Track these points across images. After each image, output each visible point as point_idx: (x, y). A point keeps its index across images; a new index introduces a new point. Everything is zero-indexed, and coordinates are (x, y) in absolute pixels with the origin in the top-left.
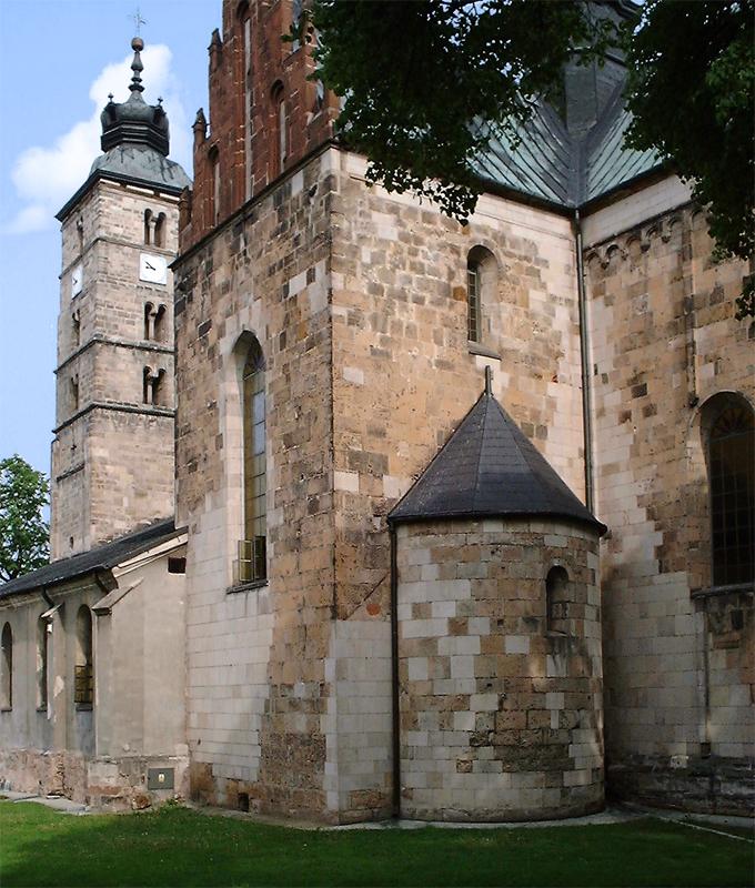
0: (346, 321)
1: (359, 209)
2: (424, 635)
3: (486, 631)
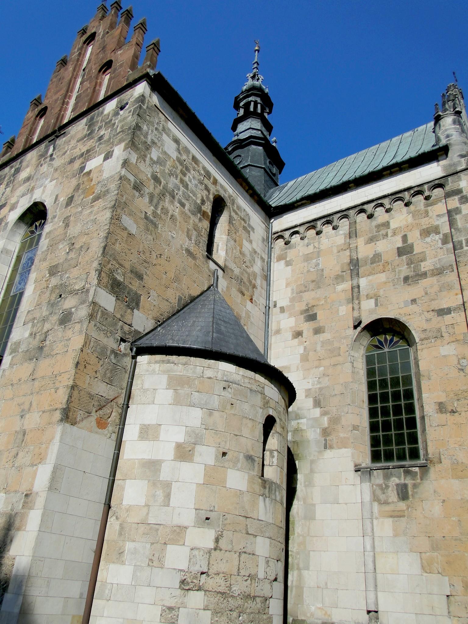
0: (132, 185)
1: (156, 126)
2: (147, 456)
3: (211, 461)
